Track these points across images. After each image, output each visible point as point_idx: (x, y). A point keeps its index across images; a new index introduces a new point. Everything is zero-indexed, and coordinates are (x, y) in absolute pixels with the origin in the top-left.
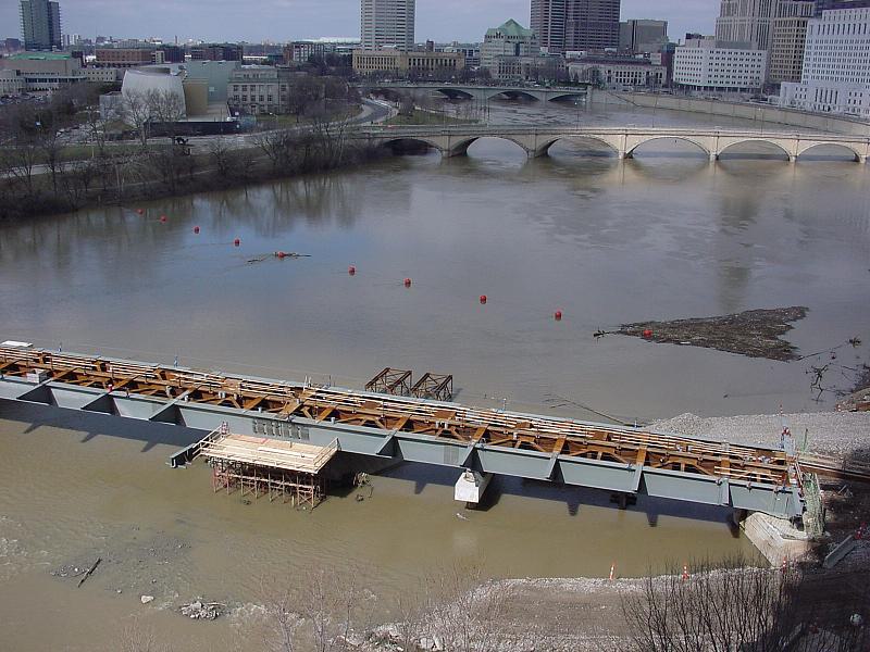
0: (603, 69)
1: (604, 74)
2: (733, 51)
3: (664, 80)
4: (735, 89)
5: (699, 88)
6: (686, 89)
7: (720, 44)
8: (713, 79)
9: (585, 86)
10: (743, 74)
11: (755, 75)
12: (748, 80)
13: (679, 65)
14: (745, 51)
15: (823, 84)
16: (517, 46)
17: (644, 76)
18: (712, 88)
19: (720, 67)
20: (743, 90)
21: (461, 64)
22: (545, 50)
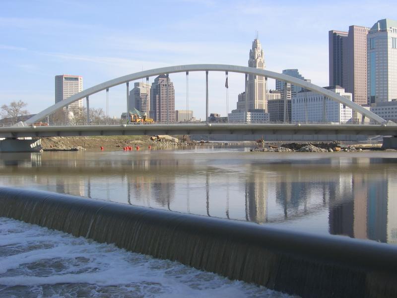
2: (259, 113)
14: (261, 113)
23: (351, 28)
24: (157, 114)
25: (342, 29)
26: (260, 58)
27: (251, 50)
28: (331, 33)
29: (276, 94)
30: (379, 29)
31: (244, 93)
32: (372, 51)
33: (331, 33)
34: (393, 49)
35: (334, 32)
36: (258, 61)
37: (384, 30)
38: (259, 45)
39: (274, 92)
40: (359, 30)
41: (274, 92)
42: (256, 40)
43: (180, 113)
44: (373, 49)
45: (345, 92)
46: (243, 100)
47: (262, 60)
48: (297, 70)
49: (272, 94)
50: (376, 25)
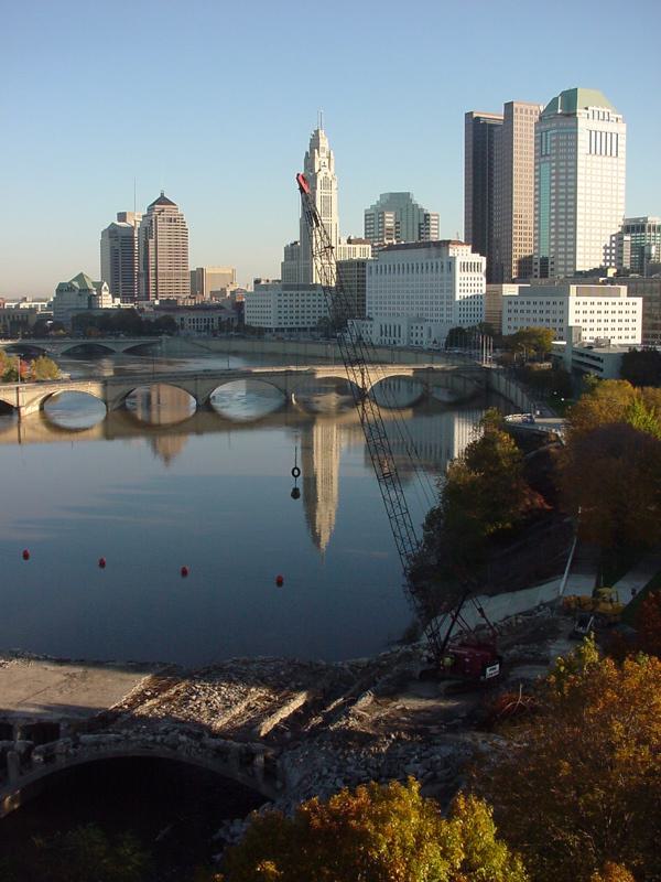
0: (177, 318)
1: (178, 321)
3: (235, 324)
4: (305, 329)
5: (270, 330)
6: (260, 332)
7: (286, 287)
8: (283, 320)
9: (161, 334)
10: (311, 314)
11: (323, 314)
12: (317, 320)
13: (250, 309)
15: (385, 321)
16: (90, 300)
17: (216, 321)
18: (283, 330)
19: (288, 309)
20: (312, 329)
21: (33, 321)
22: (118, 301)
23: (509, 107)
24: (152, 278)
25: (492, 112)
26: (324, 170)
27: (307, 153)
28: (469, 115)
29: (363, 246)
30: (560, 111)
31: (296, 243)
32: (542, 160)
33: (469, 115)
34: (589, 157)
35: (475, 115)
36: (320, 177)
37: (571, 115)
38: (324, 143)
39: (359, 241)
40: (527, 111)
41: (359, 241)
42: (317, 132)
43: (208, 271)
44: (546, 155)
45: (473, 252)
46: (292, 259)
47: (329, 176)
48: (409, 194)
49: (352, 246)
50: (553, 104)
